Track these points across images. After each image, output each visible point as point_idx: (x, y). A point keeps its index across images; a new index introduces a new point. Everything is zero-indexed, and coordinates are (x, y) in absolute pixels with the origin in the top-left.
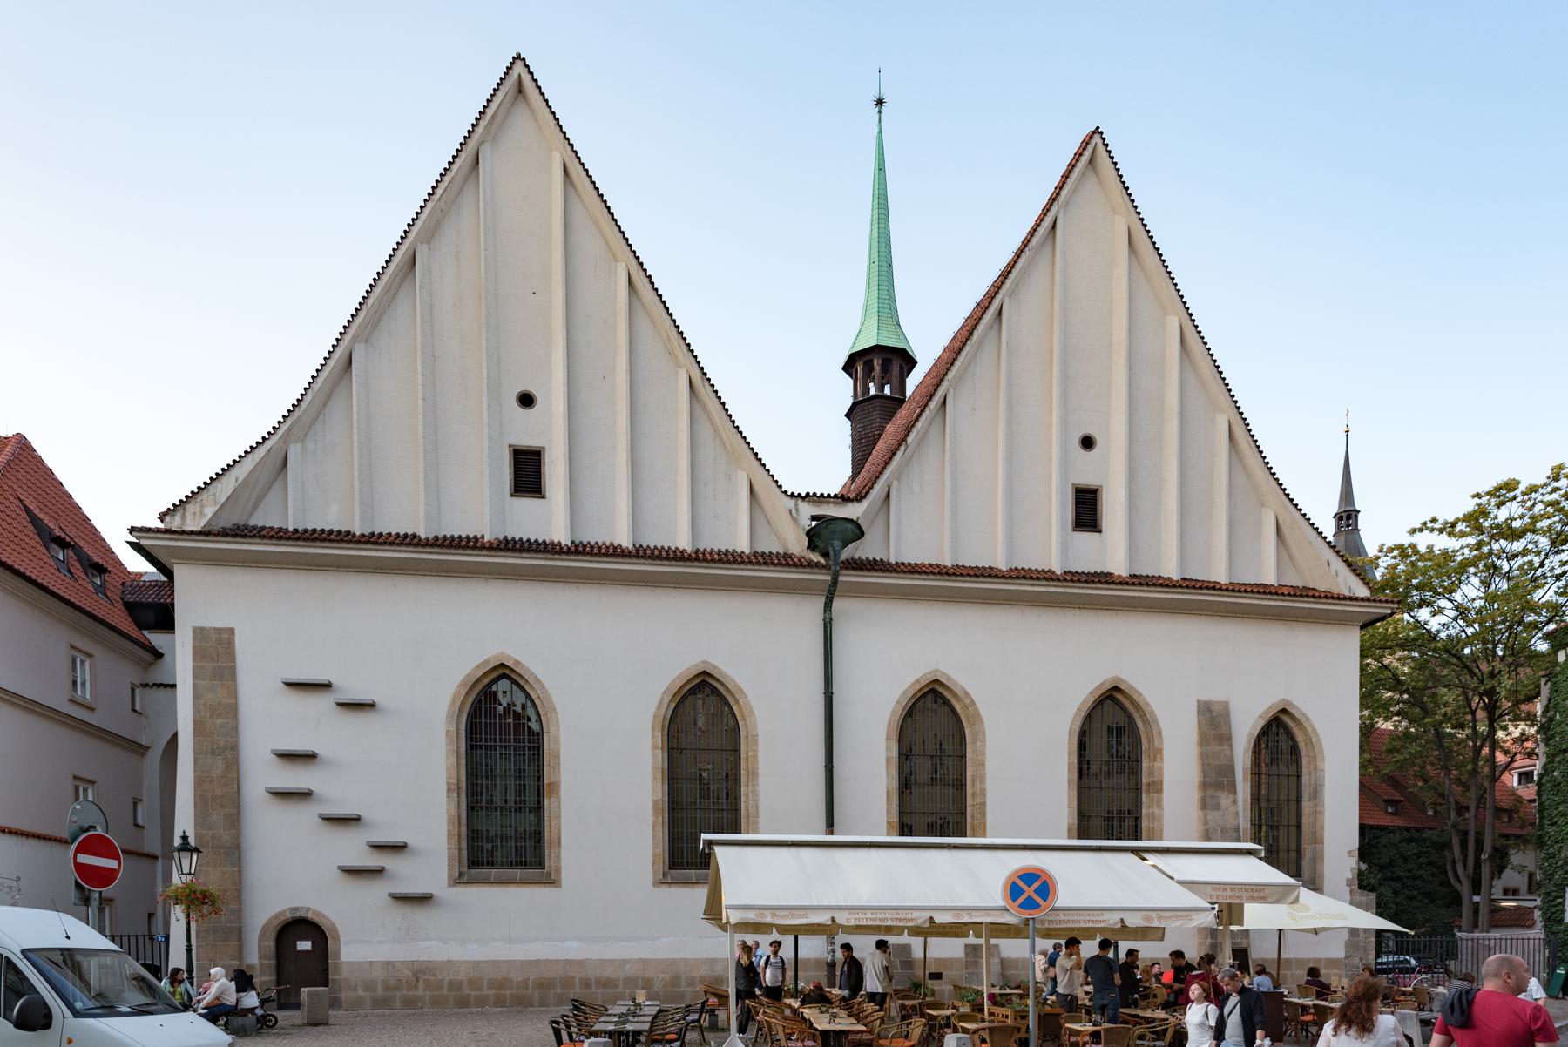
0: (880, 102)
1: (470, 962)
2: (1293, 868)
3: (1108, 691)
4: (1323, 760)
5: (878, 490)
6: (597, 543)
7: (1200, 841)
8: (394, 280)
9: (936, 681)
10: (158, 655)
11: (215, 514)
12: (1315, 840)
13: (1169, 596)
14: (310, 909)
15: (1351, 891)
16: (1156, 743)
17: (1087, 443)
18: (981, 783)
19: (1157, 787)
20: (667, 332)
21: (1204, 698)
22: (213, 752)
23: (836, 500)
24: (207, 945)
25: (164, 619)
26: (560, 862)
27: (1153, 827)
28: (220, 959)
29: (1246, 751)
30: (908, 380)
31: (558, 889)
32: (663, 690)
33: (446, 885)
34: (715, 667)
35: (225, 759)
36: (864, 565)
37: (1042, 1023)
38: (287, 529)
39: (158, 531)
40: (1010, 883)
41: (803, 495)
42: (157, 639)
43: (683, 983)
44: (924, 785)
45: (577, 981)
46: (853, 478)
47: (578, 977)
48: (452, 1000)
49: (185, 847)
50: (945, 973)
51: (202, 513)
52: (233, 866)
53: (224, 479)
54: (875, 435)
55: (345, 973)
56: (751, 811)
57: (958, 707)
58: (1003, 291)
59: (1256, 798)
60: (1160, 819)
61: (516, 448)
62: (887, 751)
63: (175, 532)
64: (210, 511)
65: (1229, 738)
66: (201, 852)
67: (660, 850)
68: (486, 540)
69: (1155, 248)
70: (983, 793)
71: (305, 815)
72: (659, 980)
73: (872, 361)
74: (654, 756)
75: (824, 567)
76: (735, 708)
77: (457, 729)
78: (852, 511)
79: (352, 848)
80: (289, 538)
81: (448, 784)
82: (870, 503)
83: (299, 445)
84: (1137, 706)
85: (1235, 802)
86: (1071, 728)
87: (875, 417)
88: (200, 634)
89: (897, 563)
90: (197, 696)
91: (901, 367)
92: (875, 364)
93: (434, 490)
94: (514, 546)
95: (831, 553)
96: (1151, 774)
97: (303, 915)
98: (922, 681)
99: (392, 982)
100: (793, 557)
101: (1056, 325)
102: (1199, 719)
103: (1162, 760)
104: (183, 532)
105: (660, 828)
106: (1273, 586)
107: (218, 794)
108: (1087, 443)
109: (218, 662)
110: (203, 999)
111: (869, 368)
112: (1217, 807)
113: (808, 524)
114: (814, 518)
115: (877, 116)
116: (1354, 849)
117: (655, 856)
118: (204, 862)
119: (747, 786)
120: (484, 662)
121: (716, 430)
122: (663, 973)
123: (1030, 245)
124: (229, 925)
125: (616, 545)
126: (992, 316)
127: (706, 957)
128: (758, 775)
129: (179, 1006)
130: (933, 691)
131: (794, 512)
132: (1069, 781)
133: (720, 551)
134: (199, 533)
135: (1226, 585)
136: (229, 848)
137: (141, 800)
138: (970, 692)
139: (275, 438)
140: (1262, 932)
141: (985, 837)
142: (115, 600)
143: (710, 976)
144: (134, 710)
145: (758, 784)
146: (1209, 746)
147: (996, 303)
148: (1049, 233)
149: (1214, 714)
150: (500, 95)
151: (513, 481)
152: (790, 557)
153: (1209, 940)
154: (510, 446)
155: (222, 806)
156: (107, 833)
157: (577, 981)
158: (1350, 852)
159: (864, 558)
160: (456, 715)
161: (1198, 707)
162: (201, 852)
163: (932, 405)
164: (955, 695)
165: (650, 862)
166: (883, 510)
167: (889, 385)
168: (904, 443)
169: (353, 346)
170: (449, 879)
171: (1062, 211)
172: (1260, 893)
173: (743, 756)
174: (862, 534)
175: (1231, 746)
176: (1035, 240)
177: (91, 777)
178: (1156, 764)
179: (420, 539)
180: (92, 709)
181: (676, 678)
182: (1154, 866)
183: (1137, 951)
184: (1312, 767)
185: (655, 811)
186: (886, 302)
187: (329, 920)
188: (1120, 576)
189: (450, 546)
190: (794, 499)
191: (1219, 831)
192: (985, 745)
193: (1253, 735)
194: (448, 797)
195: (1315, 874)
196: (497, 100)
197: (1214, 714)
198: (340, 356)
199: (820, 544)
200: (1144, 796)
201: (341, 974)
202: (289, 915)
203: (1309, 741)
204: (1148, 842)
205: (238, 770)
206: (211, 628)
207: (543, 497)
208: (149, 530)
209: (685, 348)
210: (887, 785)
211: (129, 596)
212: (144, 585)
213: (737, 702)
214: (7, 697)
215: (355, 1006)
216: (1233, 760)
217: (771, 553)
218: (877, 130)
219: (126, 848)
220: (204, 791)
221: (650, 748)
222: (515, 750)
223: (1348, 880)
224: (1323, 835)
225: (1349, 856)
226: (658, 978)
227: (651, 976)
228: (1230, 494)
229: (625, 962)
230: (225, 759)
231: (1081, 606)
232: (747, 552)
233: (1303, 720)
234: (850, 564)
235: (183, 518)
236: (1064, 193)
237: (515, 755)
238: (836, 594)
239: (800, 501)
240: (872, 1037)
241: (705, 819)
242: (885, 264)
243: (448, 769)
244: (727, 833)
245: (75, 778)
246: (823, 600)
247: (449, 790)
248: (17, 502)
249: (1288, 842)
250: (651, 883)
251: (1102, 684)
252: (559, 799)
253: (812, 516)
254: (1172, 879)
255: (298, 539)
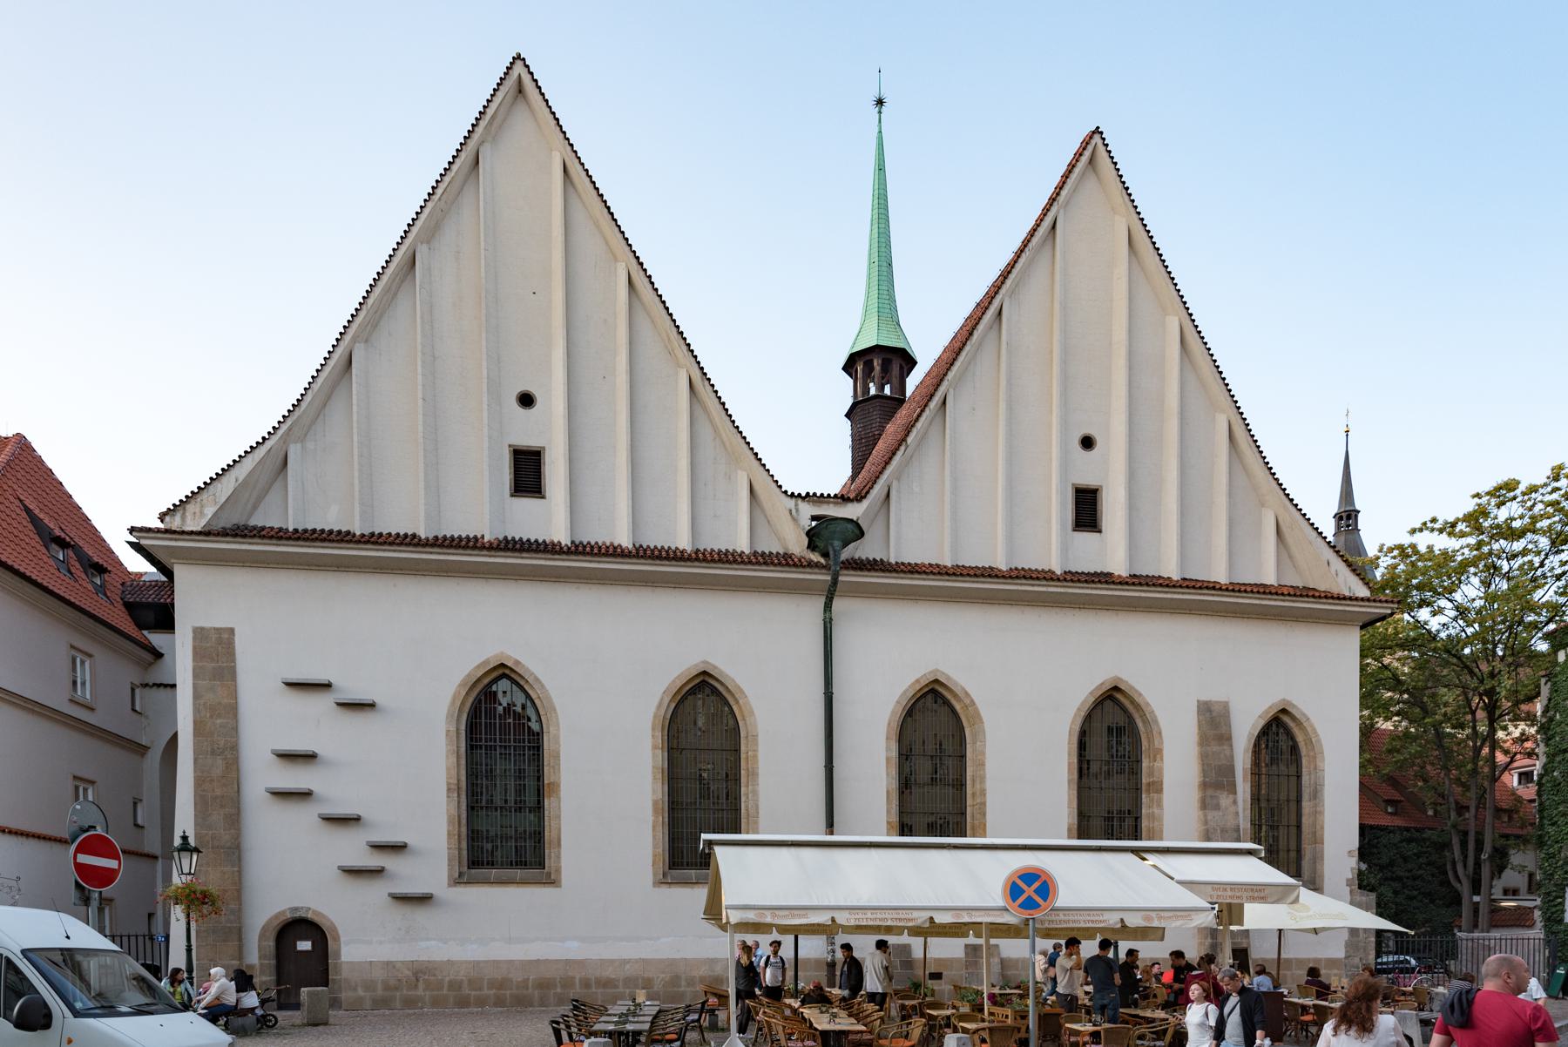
0: (880, 102)
1: (470, 962)
2: (1293, 868)
3: (1108, 691)
4: (1323, 760)
5: (878, 490)
6: (597, 543)
7: (1200, 841)
8: (394, 280)
9: (936, 681)
10: (158, 655)
11: (215, 514)
12: (1315, 840)
13: (1169, 596)
14: (310, 909)
15: (1351, 891)
16: (1156, 743)
17: (1087, 443)
18: (981, 783)
19: (1157, 787)
20: (667, 332)
21: (1204, 698)
22: (213, 752)
23: (836, 500)
24: (207, 945)
25: (164, 619)
26: (560, 862)
27: (1153, 827)
28: (220, 959)
29: (1246, 751)
30: (908, 380)
31: (558, 889)
32: (663, 690)
33: (446, 885)
34: (715, 667)
35: (225, 759)
36: (864, 565)
37: (1042, 1023)
38: (287, 529)
39: (158, 531)
40: (1010, 883)
41: (803, 495)
42: (157, 639)
43: (683, 983)
44: (924, 785)
45: (577, 981)
46: (853, 478)
47: (578, 977)
48: (452, 1000)
49: (185, 847)
50: (945, 973)
51: (202, 513)
52: (233, 866)
53: (224, 479)
54: (875, 435)
55: (345, 973)
56: (751, 811)
57: (958, 707)
58: (1003, 291)
59: (1256, 798)
60: (1160, 819)
61: (516, 448)
62: (887, 751)
63: (175, 532)
64: (210, 511)
65: (1229, 738)
66: (201, 852)
67: (660, 850)
68: (486, 540)
69: (1155, 248)
70: (983, 793)
71: (305, 815)
72: (659, 980)
73: (872, 361)
74: (654, 756)
75: (824, 567)
76: (735, 708)
77: (457, 729)
78: (852, 511)
79: (352, 848)
80: (289, 538)
81: (448, 784)
82: (870, 503)
83: (299, 445)
84: (1137, 706)
85: (1235, 802)
86: (1071, 728)
87: (875, 417)
88: (200, 634)
89: (897, 563)
90: (197, 696)
91: (901, 367)
92: (875, 364)
93: (434, 490)
94: (514, 546)
95: (831, 553)
96: (1151, 774)
97: (303, 915)
98: (922, 681)
99: (392, 982)
100: (793, 557)
101: (1056, 325)
102: (1199, 719)
103: (1162, 760)
104: (183, 532)
105: (660, 828)
106: (1273, 586)
107: (218, 794)
108: (1087, 443)
109: (218, 662)
110: (203, 999)
111: (869, 368)
112: (1217, 807)
113: (808, 524)
114: (814, 518)
115: (877, 116)
116: (1354, 849)
117: (655, 856)
118: (204, 862)
119: (747, 786)
120: (484, 662)
121: (716, 430)
122: (663, 973)
123: (1030, 245)
124: (229, 925)
125: (616, 545)
126: (992, 316)
127: (706, 957)
128: (758, 775)
129: (179, 1006)
130: (933, 691)
131: (794, 512)
132: (1069, 781)
133: (720, 551)
134: (199, 533)
135: (1226, 585)
136: (229, 848)
137: (141, 800)
138: (970, 692)
139: (275, 438)
140: (1262, 932)
141: (985, 837)
142: (115, 600)
143: (710, 976)
144: (134, 710)
145: (758, 784)
146: (1209, 746)
147: (996, 303)
148: (1049, 233)
149: (1214, 714)
150: (500, 95)
151: (513, 481)
152: (790, 557)
153: (1209, 940)
154: (510, 446)
155: (222, 806)
156: (107, 833)
157: (577, 981)
158: (1350, 852)
159: (864, 558)
160: (456, 715)
161: (1198, 707)
162: (201, 852)
163: (932, 405)
164: (955, 695)
165: (650, 862)
166: (883, 510)
167: (889, 385)
168: (904, 443)
169: (353, 346)
170: (449, 879)
171: (1062, 211)
172: (1260, 893)
173: (743, 756)
174: (862, 534)
175: (1231, 746)
176: (1035, 240)
177: (91, 777)
178: (1156, 764)
179: (420, 539)
180: (92, 709)
181: (676, 678)
182: (1154, 866)
183: (1137, 951)
184: (1312, 767)
185: (655, 811)
186: (886, 302)
187: (329, 920)
188: (1120, 576)
189: (450, 546)
190: (794, 499)
191: (1219, 831)
192: (985, 745)
193: (1253, 735)
194: (448, 797)
195: (1315, 874)
196: (497, 100)
197: (1214, 714)
198: (340, 356)
199: (820, 544)
200: (1144, 796)
201: (341, 974)
202: (289, 915)
203: (1309, 741)
204: (1148, 842)
205: (238, 770)
206: (211, 628)
207: (543, 497)
208: (149, 530)
209: (685, 348)
210: (887, 785)
211: (129, 596)
212: (144, 585)
213: (737, 702)
214: (7, 697)
215: (355, 1006)
216: (1233, 760)
217: (771, 553)
218: (877, 130)
219: (126, 848)
220: (204, 791)
221: (650, 748)
222: (515, 750)
223: (1348, 880)
224: (1323, 835)
225: (1349, 856)
226: (658, 978)
227: (651, 976)
228: (1230, 494)
229: (625, 962)
230: (225, 759)
231: (1081, 606)
232: (747, 552)
233: (1303, 720)
234: (850, 564)
235: (183, 518)
236: (1064, 193)
237: (515, 755)
238: (836, 594)
239: (800, 501)
240: (872, 1037)
241: (705, 819)
242: (885, 264)
243: (448, 769)
244: (727, 833)
245: (75, 778)
246: (823, 600)
247: (449, 790)
248: (17, 502)
249: (1288, 842)
250: (651, 883)
251: (1102, 684)
252: (559, 799)
253: (812, 516)
254: (1172, 879)
255: (298, 539)
